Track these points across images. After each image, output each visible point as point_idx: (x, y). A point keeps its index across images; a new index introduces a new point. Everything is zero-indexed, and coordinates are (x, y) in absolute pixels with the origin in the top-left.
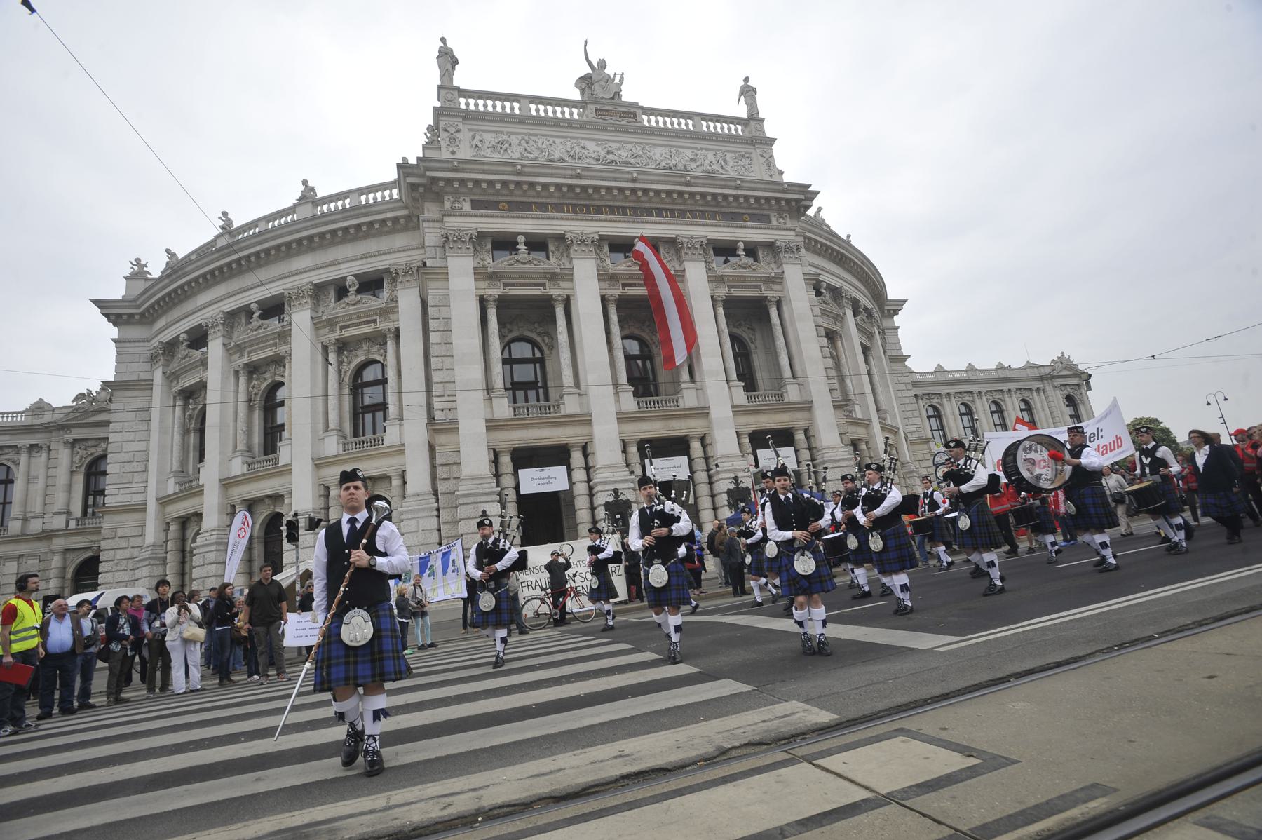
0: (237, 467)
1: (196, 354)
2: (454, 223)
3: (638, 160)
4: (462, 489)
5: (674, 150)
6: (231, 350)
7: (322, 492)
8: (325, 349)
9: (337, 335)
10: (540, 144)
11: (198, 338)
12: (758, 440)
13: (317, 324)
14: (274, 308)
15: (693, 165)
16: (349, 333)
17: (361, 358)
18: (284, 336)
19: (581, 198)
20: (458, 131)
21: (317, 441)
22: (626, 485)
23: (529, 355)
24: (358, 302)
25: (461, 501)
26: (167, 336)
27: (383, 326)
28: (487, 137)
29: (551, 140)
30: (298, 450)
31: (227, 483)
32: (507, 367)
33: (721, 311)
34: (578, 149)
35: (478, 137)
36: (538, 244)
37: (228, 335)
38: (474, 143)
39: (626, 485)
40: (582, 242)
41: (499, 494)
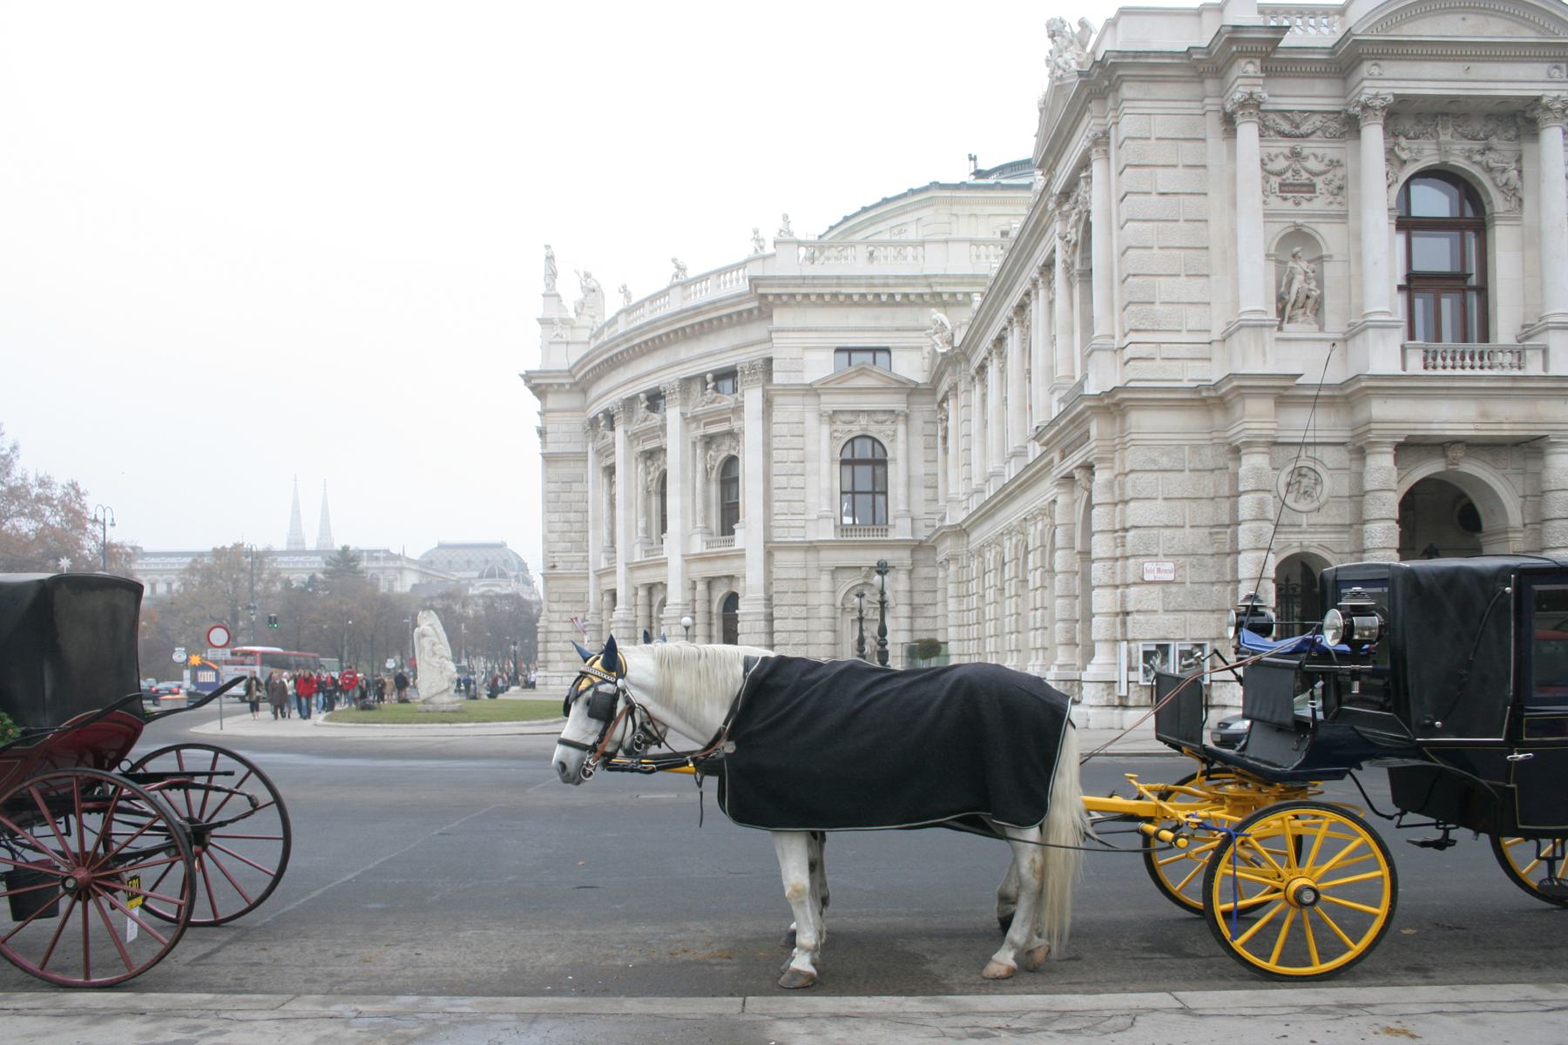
0: (638, 557)
1: (609, 433)
6: (632, 438)
7: (690, 584)
8: (694, 444)
9: (701, 432)
11: (610, 418)
13: (687, 420)
14: (655, 399)
16: (713, 430)
17: (724, 455)
18: (663, 428)
21: (686, 538)
23: (870, 456)
24: (713, 402)
26: (591, 414)
27: (736, 425)
30: (672, 548)
31: (633, 568)
32: (847, 470)
37: (629, 420)
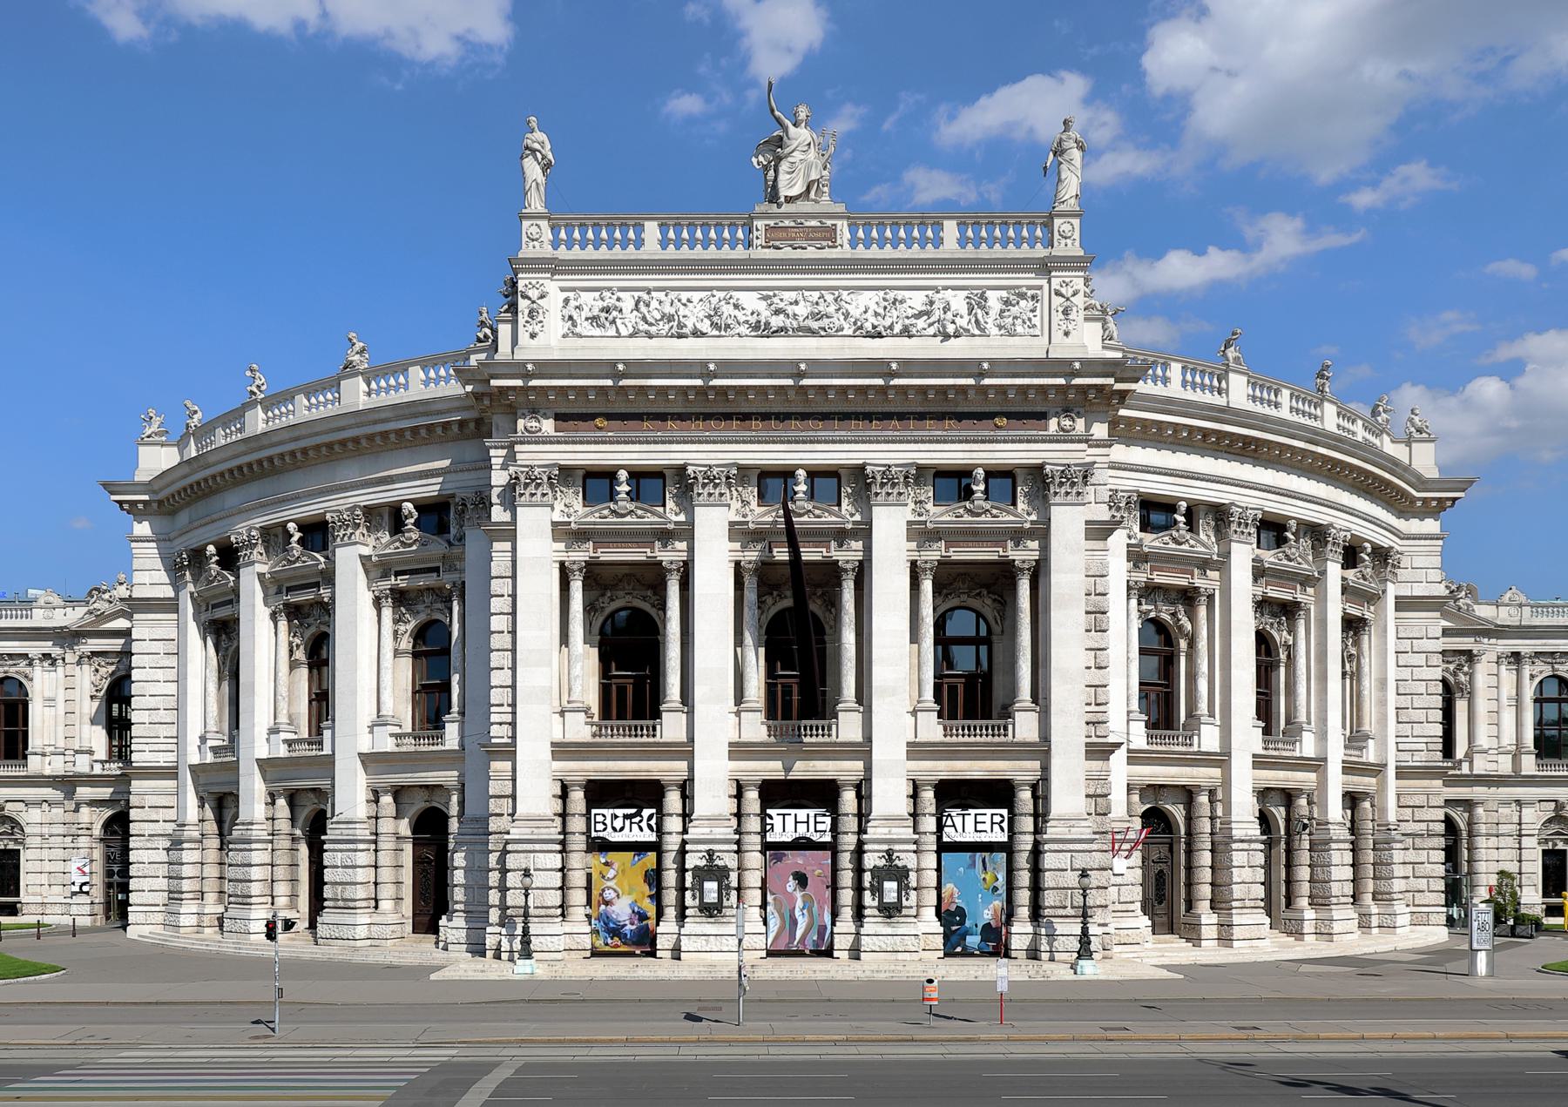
2: (528, 455)
3: (825, 322)
4: (515, 833)
5: (891, 295)
10: (668, 309)
12: (954, 794)
15: (921, 323)
19: (716, 405)
20: (542, 297)
22: (726, 847)
25: (509, 847)
28: (587, 298)
29: (684, 296)
33: (927, 586)
34: (727, 310)
35: (573, 303)
36: (647, 482)
38: (566, 313)
39: (726, 847)
40: (711, 480)
41: (563, 843)
